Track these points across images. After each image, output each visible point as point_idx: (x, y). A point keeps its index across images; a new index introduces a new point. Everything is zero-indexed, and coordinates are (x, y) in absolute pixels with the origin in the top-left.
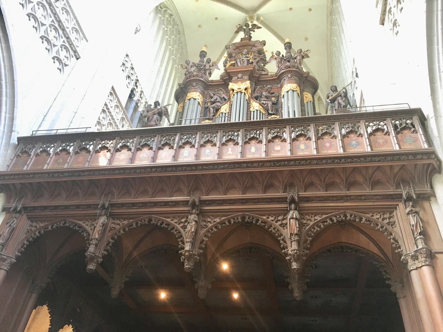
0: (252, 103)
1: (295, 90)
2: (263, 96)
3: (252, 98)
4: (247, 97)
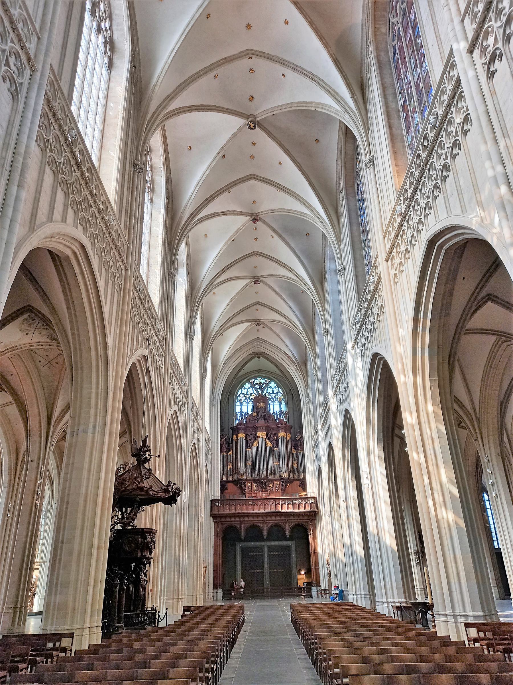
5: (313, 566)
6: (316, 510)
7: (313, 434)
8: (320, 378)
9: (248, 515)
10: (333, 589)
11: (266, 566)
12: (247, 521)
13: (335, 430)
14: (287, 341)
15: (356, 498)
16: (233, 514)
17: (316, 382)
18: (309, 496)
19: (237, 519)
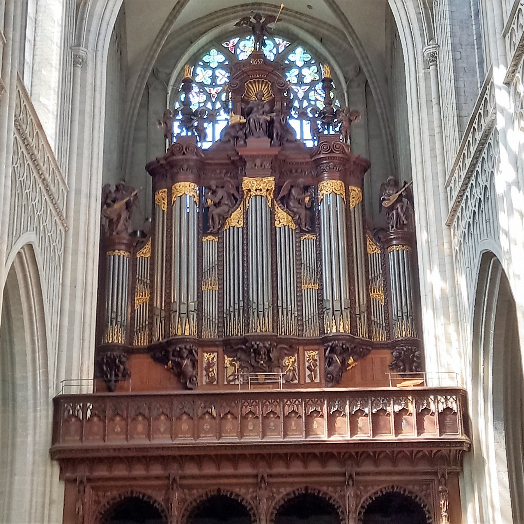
0: (277, 210)
1: (338, 193)
2: (292, 197)
3: (277, 201)
4: (269, 204)
6: (464, 438)
12: (193, 477)
19: (157, 470)
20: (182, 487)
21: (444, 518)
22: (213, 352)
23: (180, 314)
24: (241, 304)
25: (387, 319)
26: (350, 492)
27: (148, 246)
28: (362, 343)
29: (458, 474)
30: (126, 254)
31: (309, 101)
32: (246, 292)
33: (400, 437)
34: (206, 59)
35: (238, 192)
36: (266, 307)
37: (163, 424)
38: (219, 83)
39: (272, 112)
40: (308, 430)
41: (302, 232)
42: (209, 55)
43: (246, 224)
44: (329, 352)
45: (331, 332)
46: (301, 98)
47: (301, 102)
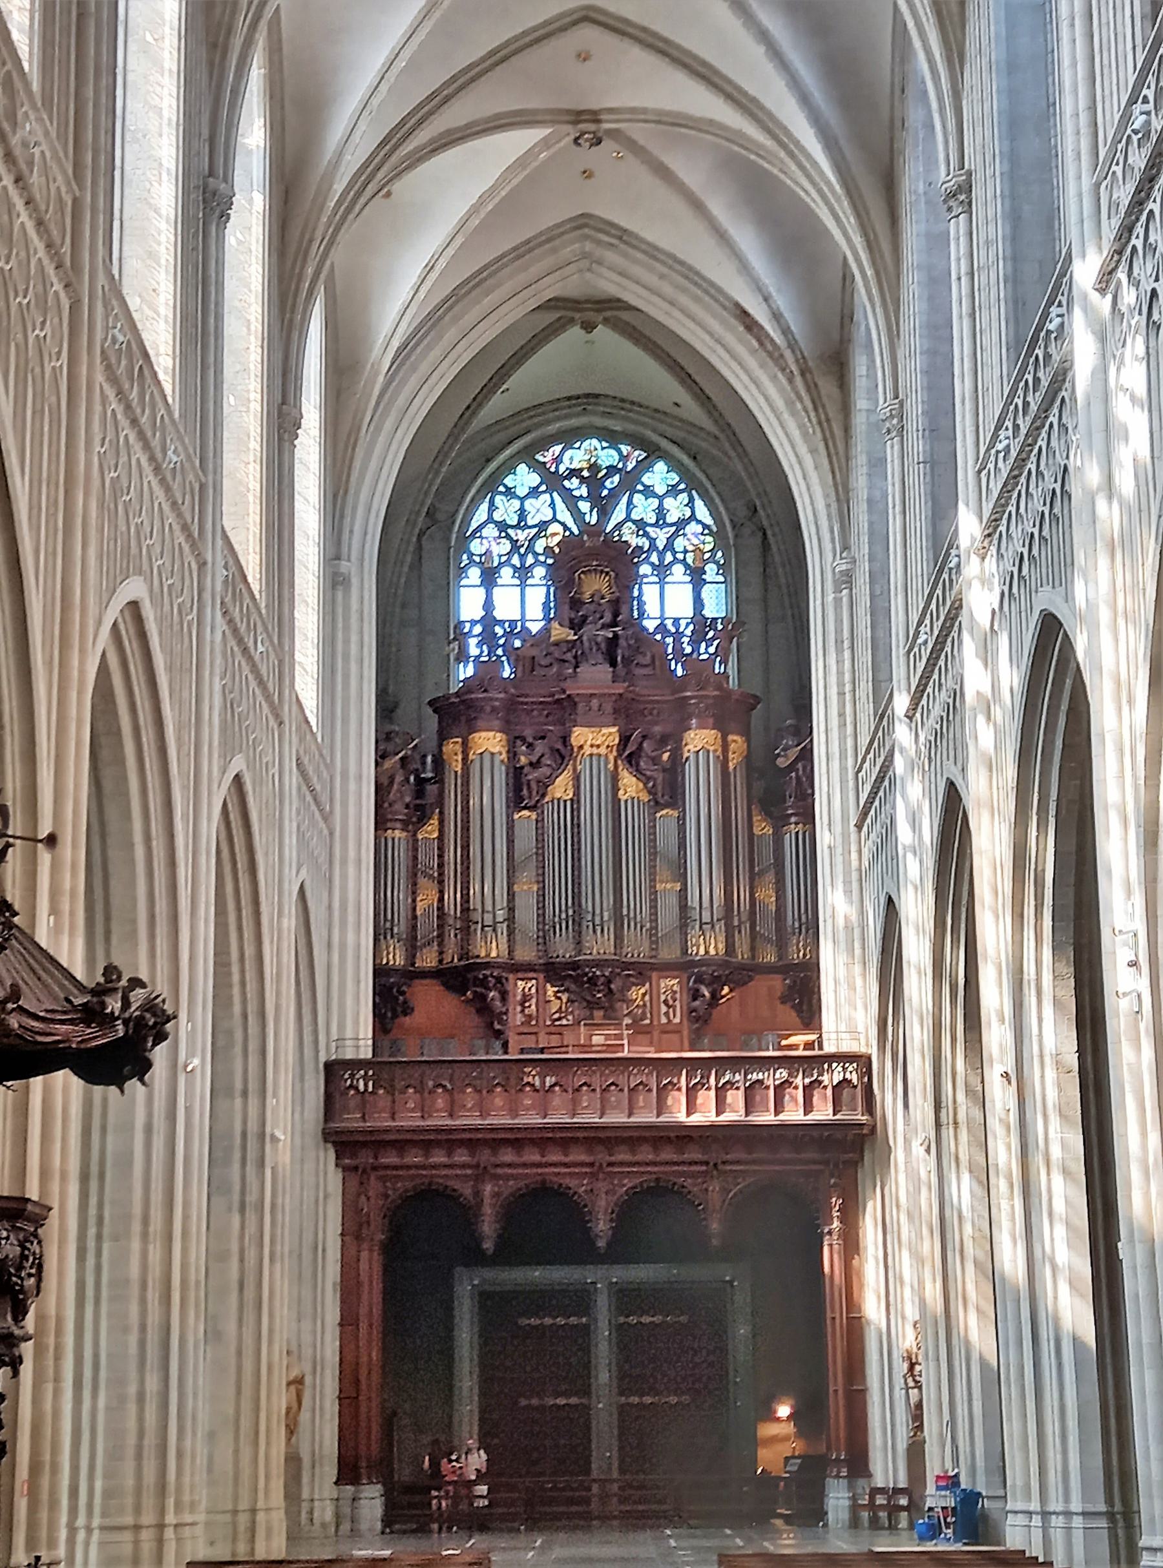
1: (712, 748)
4: (611, 766)
5: (836, 1384)
7: (864, 741)
8: (917, 446)
9: (518, 1139)
10: (931, 1489)
11: (603, 1376)
12: (509, 1165)
13: (981, 719)
14: (747, 240)
15: (1073, 1060)
16: (438, 1130)
17: (893, 467)
18: (829, 1048)
19: (461, 1156)
20: (496, 1177)
21: (835, 1220)
22: (531, 979)
23: (483, 927)
24: (570, 912)
25: (778, 930)
26: (715, 1186)
27: (435, 821)
28: (742, 967)
29: (856, 1163)
30: (405, 834)
31: (674, 553)
32: (577, 896)
33: (781, 1117)
34: (509, 481)
35: (566, 746)
36: (606, 918)
37: (469, 1097)
38: (530, 522)
39: (614, 624)
40: (661, 1109)
41: (657, 805)
42: (514, 473)
43: (577, 793)
44: (695, 982)
45: (697, 954)
46: (661, 548)
47: (661, 555)
